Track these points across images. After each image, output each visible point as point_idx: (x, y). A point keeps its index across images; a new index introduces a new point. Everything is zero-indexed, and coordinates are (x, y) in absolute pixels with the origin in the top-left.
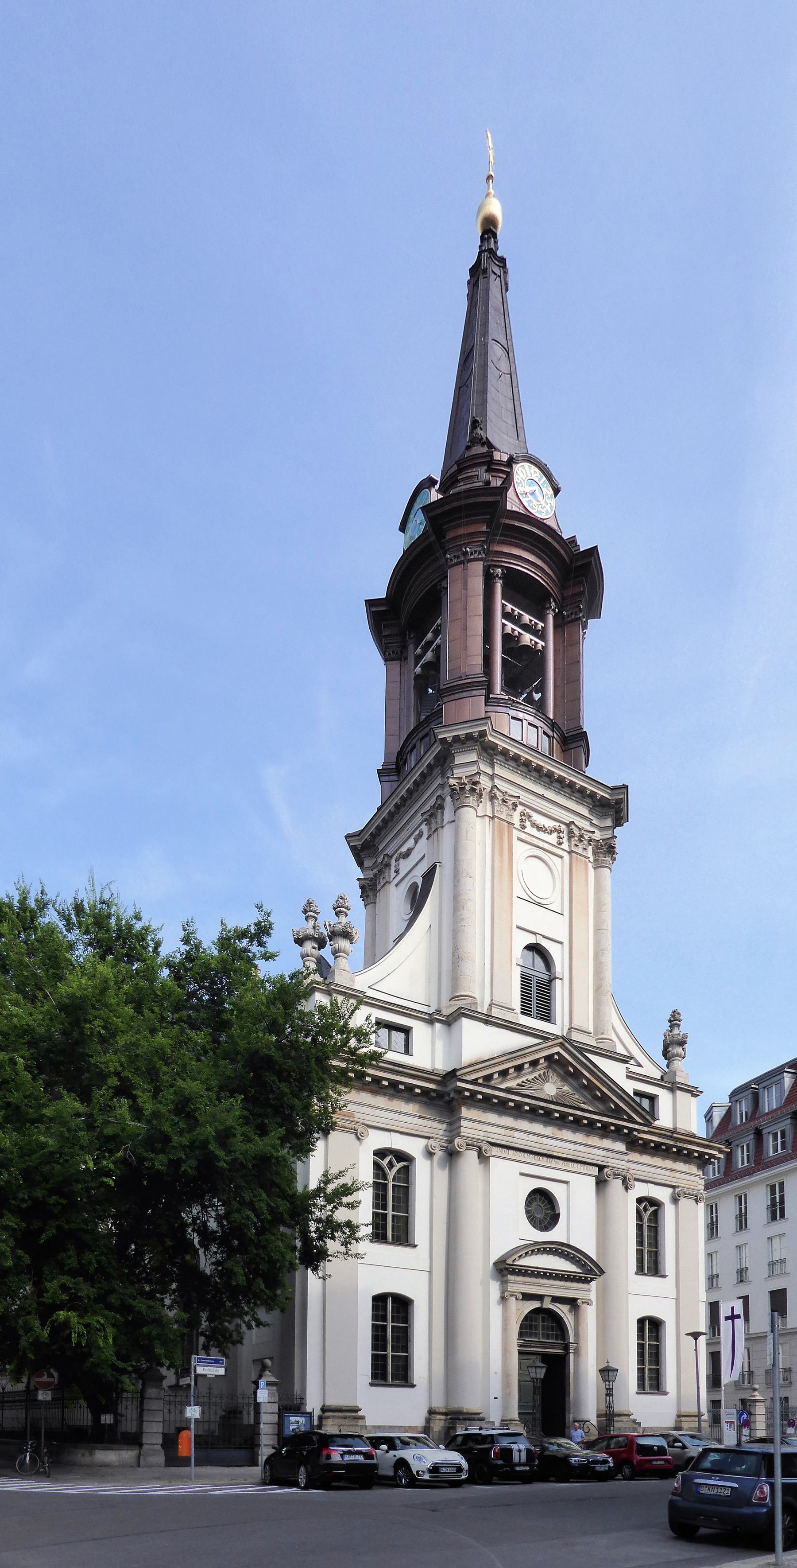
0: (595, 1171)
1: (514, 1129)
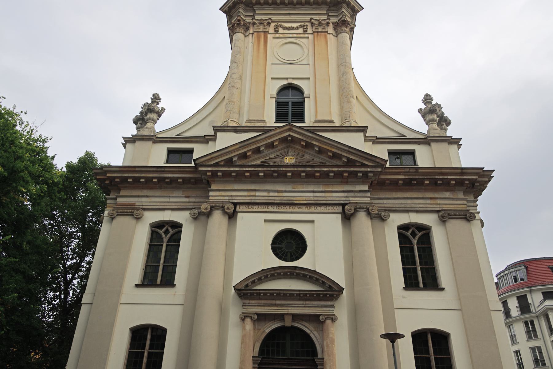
0: (340, 209)
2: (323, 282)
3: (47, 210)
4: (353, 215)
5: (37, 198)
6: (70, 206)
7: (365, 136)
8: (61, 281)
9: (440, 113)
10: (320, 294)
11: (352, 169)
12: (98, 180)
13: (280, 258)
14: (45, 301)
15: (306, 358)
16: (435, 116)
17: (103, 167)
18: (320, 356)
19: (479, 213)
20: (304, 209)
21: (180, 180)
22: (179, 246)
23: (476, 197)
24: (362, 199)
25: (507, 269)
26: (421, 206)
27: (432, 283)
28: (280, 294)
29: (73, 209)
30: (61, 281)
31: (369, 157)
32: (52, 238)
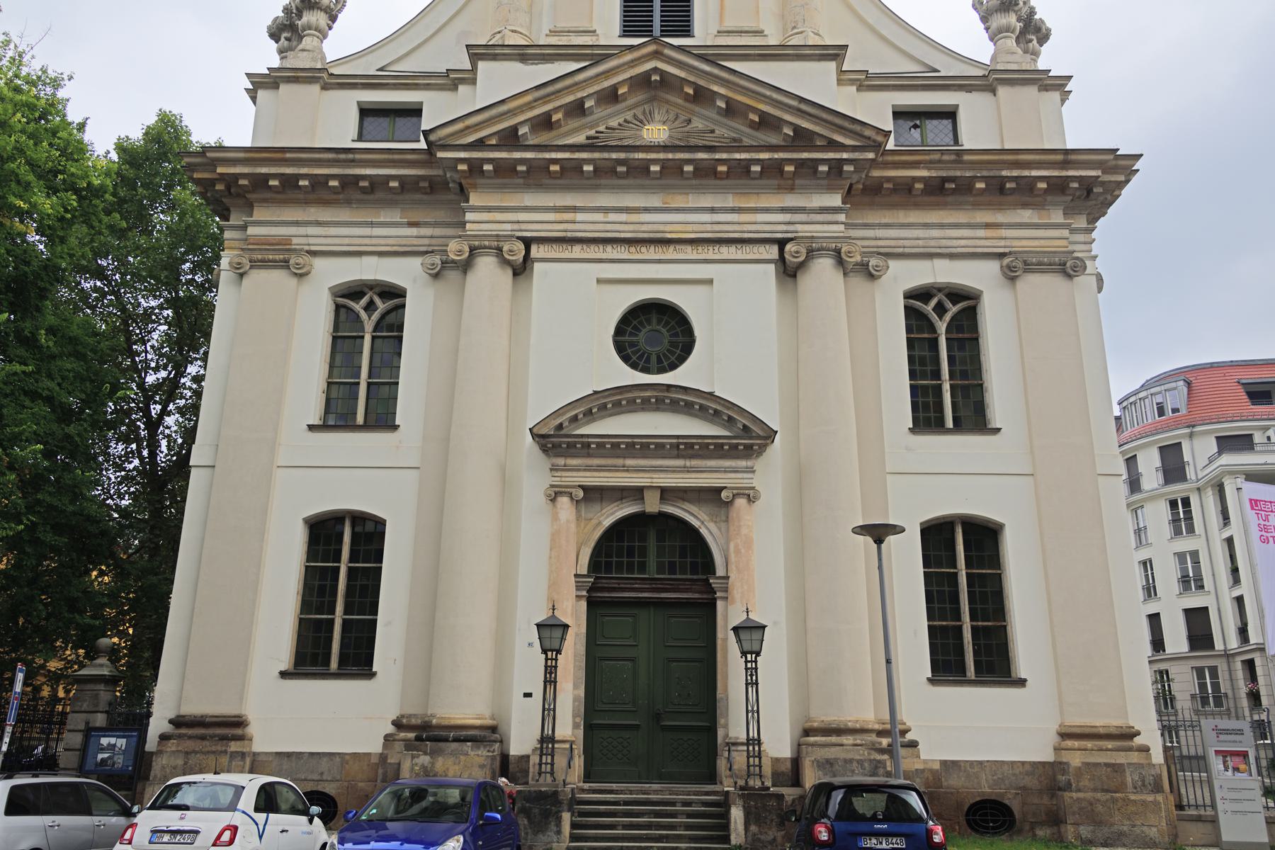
0: (773, 252)
1: (575, 209)
2: (730, 418)
3: (83, 256)
4: (801, 265)
5: (57, 224)
6: (138, 248)
7: (841, 72)
8: (138, 420)
9: (1024, 10)
10: (723, 445)
11: (805, 155)
12: (197, 182)
13: (634, 366)
14: (108, 462)
15: (689, 577)
16: (1012, 19)
17: (205, 149)
18: (720, 571)
19: (1094, 258)
20: (689, 252)
21: (394, 184)
22: (400, 339)
23: (1093, 220)
24: (826, 228)
25: (1144, 387)
26: (963, 242)
27: (973, 417)
28: (634, 444)
29: (145, 252)
30: (138, 420)
31: (846, 124)
32: (106, 321)
